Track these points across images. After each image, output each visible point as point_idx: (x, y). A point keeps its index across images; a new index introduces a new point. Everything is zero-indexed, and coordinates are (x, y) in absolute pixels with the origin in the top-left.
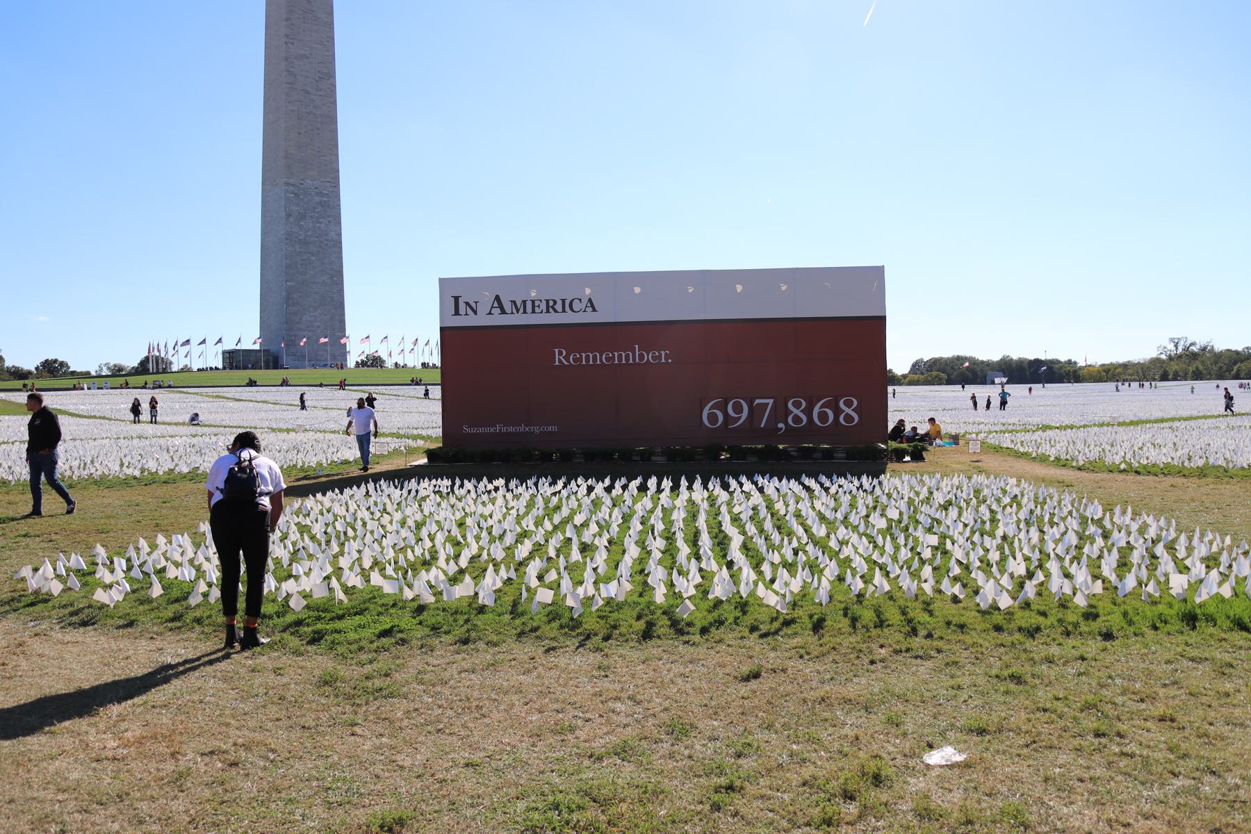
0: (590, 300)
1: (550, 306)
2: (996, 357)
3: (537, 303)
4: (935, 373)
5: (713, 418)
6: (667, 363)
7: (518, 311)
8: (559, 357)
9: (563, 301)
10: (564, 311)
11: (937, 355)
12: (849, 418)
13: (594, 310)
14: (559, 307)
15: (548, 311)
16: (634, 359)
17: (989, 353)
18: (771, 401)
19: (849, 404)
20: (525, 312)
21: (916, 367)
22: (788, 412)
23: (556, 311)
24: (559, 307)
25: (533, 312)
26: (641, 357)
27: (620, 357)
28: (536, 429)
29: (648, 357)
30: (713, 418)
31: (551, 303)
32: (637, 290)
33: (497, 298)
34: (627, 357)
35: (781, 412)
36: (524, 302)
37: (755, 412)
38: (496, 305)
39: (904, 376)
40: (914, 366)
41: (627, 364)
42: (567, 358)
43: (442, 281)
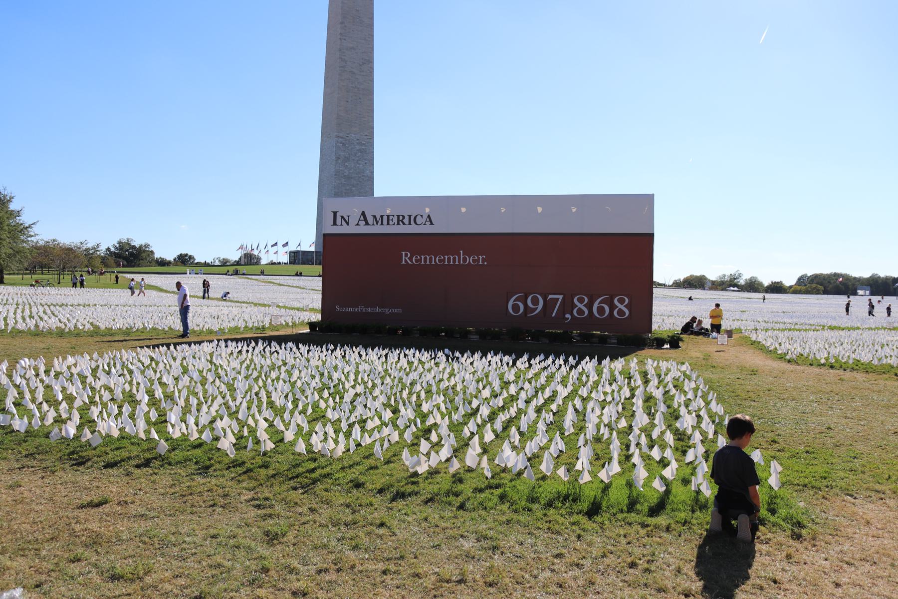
0: (429, 216)
1: (400, 220)
2: (866, 275)
3: (391, 218)
4: (814, 285)
5: (516, 308)
9: (410, 216)
10: (410, 224)
11: (818, 272)
13: (432, 224)
14: (406, 221)
15: (398, 224)
16: (459, 261)
17: (860, 268)
18: (561, 297)
20: (382, 224)
21: (801, 280)
22: (573, 306)
23: (404, 224)
24: (406, 221)
25: (388, 224)
27: (449, 259)
28: (387, 311)
29: (469, 260)
30: (516, 308)
31: (401, 218)
32: (463, 210)
33: (363, 213)
34: (454, 259)
35: (568, 305)
39: (791, 287)
40: (799, 279)
41: (454, 265)
42: (411, 259)
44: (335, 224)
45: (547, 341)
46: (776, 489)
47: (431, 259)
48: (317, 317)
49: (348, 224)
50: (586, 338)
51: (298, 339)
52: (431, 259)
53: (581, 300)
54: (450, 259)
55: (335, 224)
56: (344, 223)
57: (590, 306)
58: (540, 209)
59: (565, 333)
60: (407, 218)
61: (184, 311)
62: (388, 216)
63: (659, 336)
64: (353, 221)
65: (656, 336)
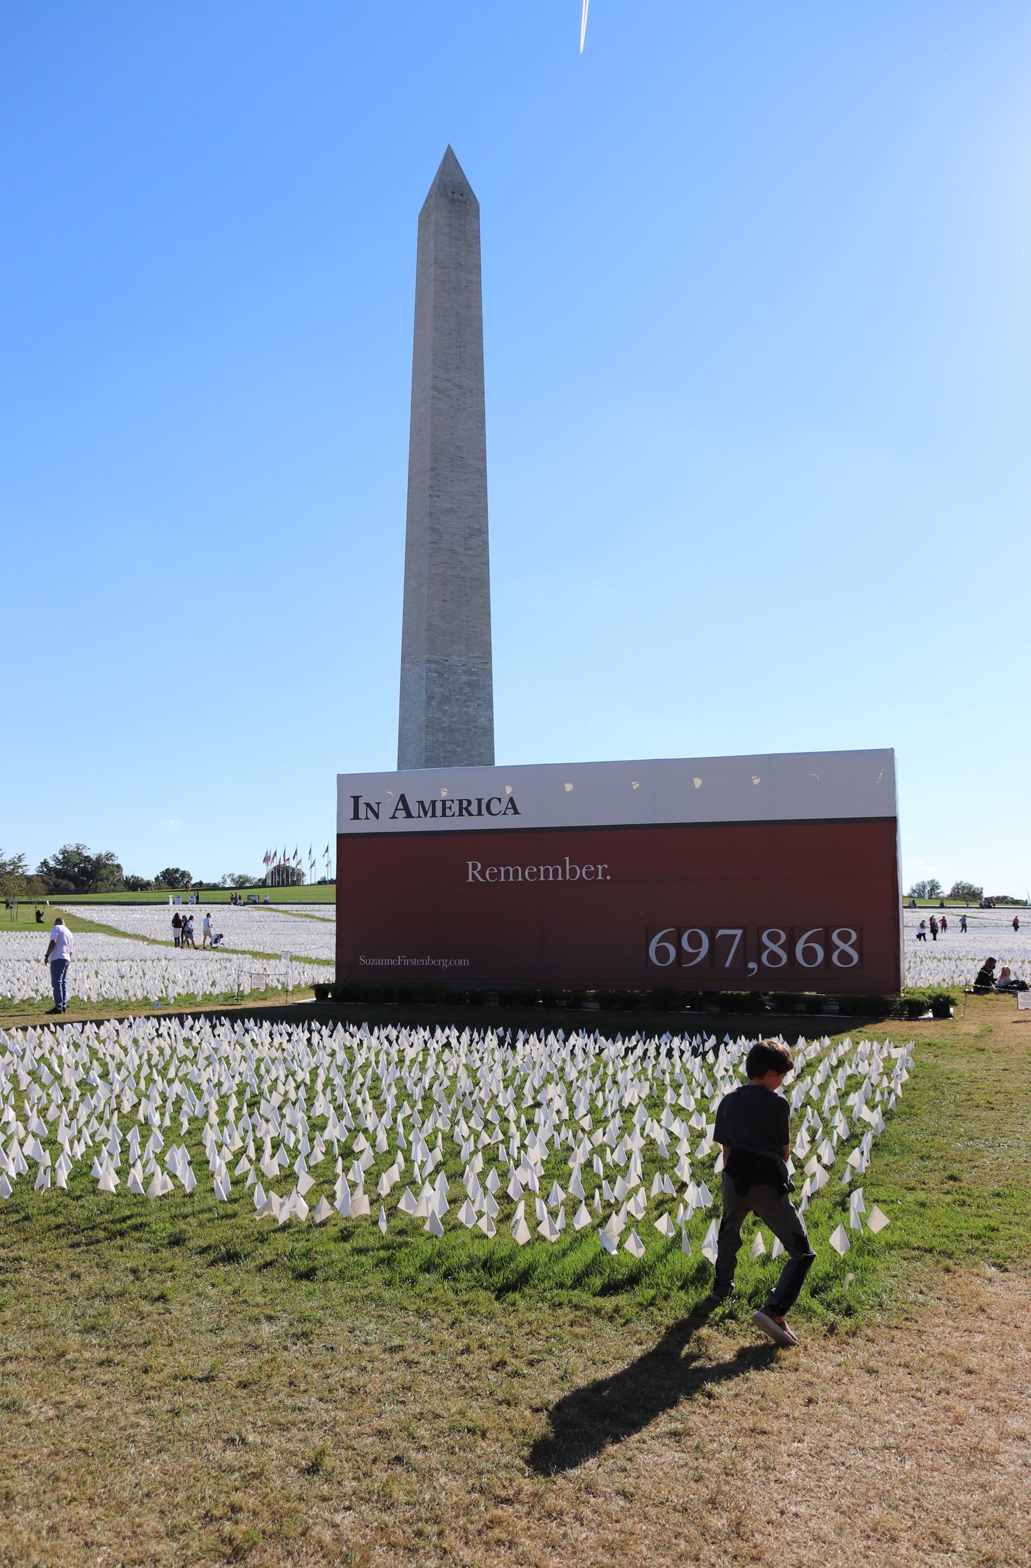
0: (511, 800)
1: (464, 808)
6: (605, 880)
7: (426, 814)
8: (473, 872)
9: (480, 801)
10: (480, 813)
12: (845, 957)
13: (516, 812)
14: (474, 809)
15: (461, 814)
19: (845, 937)
20: (434, 815)
22: (762, 947)
23: (470, 814)
24: (474, 809)
25: (444, 815)
26: (573, 872)
28: (444, 963)
29: (582, 873)
32: (569, 787)
33: (403, 798)
34: (556, 871)
35: (751, 948)
36: (433, 803)
37: (718, 947)
38: (401, 806)
41: (555, 881)
42: (482, 873)
43: (340, 777)
44: (356, 817)
45: (716, 1010)
46: (842, 1253)
47: (516, 872)
48: (327, 975)
49: (377, 816)
50: (787, 1004)
51: (293, 1015)
52: (516, 872)
53: (774, 938)
54: (547, 872)
55: (356, 817)
56: (370, 814)
57: (789, 948)
58: (698, 782)
59: (755, 995)
60: (475, 803)
61: (59, 968)
62: (444, 802)
63: (916, 997)
64: (385, 812)
65: (909, 997)
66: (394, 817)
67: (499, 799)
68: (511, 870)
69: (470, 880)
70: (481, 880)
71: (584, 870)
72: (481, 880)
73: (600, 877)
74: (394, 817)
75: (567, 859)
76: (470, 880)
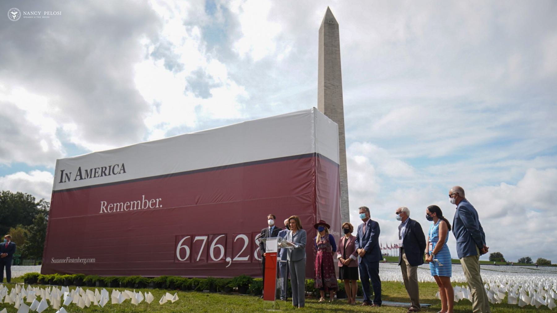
0: (123, 165)
7: (88, 176)
10: (109, 174)
13: (124, 172)
15: (102, 176)
23: (105, 175)
24: (107, 172)
25: (95, 177)
31: (104, 169)
36: (91, 170)
42: (106, 208)
66: (75, 180)
67: (118, 165)
68: (119, 205)
69: (101, 212)
70: (106, 211)
71: (150, 202)
72: (106, 211)
73: (157, 206)
74: (75, 180)
75: (144, 196)
76: (101, 212)
